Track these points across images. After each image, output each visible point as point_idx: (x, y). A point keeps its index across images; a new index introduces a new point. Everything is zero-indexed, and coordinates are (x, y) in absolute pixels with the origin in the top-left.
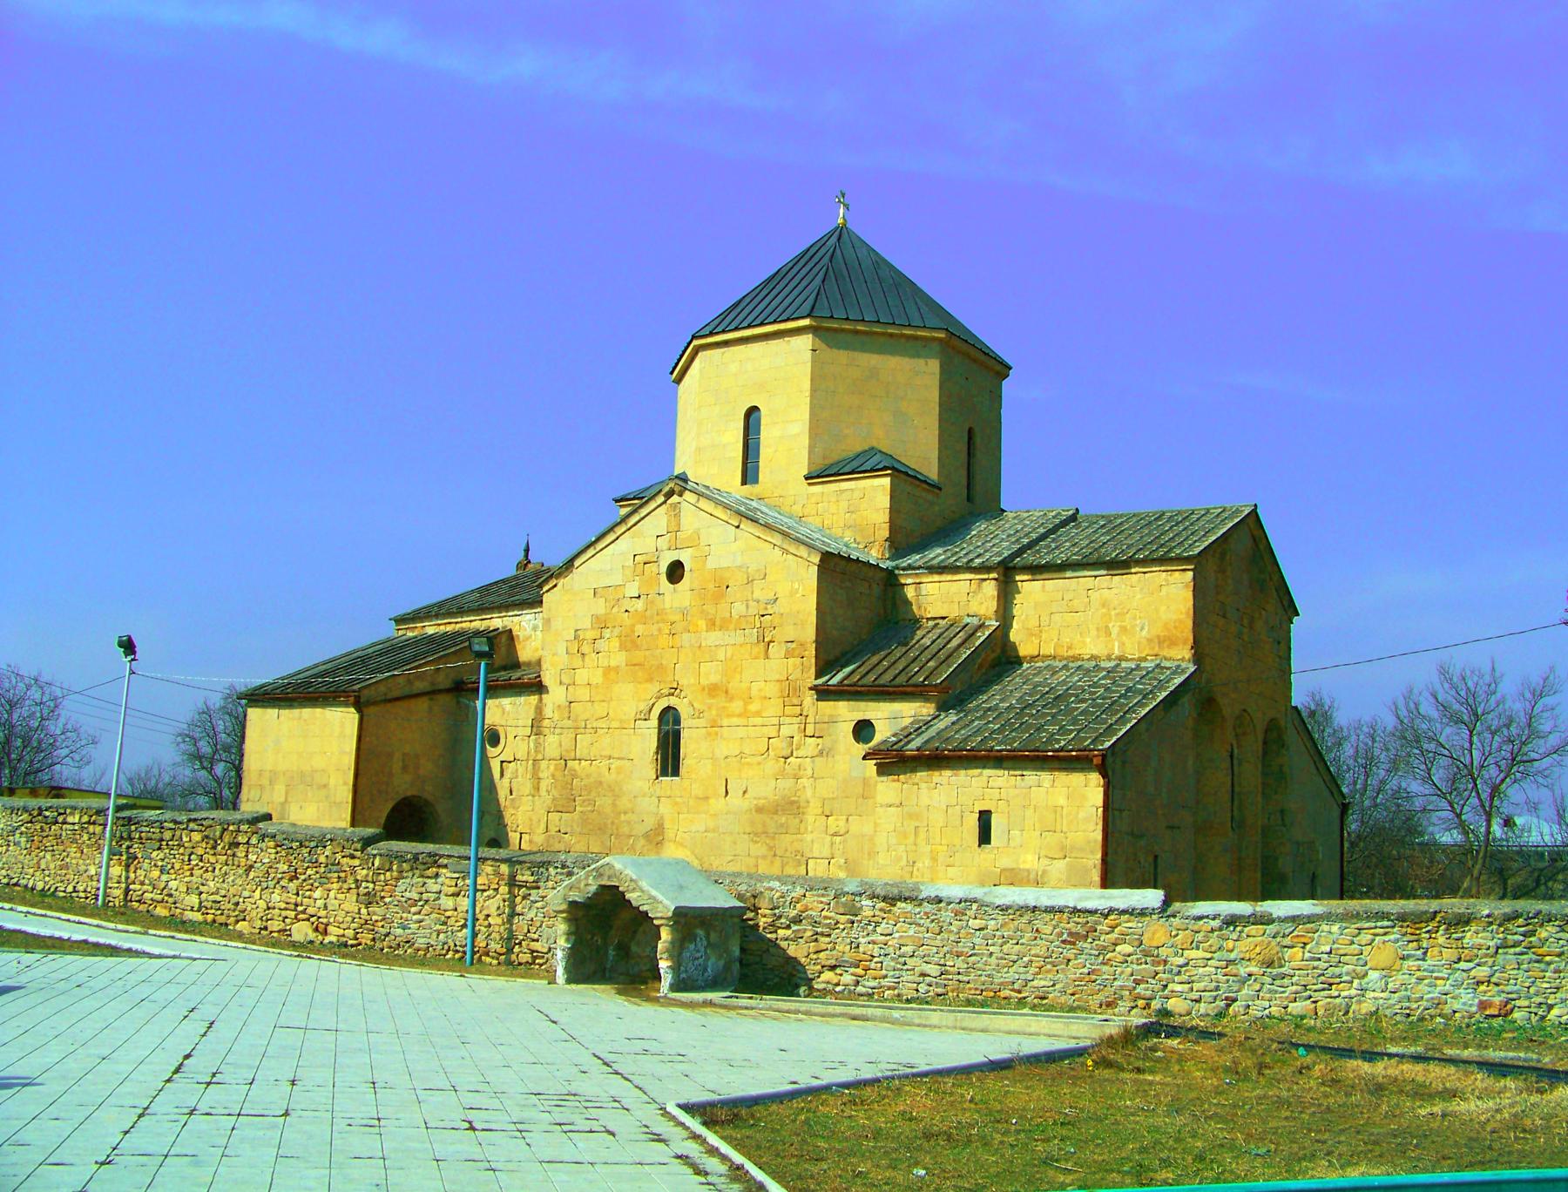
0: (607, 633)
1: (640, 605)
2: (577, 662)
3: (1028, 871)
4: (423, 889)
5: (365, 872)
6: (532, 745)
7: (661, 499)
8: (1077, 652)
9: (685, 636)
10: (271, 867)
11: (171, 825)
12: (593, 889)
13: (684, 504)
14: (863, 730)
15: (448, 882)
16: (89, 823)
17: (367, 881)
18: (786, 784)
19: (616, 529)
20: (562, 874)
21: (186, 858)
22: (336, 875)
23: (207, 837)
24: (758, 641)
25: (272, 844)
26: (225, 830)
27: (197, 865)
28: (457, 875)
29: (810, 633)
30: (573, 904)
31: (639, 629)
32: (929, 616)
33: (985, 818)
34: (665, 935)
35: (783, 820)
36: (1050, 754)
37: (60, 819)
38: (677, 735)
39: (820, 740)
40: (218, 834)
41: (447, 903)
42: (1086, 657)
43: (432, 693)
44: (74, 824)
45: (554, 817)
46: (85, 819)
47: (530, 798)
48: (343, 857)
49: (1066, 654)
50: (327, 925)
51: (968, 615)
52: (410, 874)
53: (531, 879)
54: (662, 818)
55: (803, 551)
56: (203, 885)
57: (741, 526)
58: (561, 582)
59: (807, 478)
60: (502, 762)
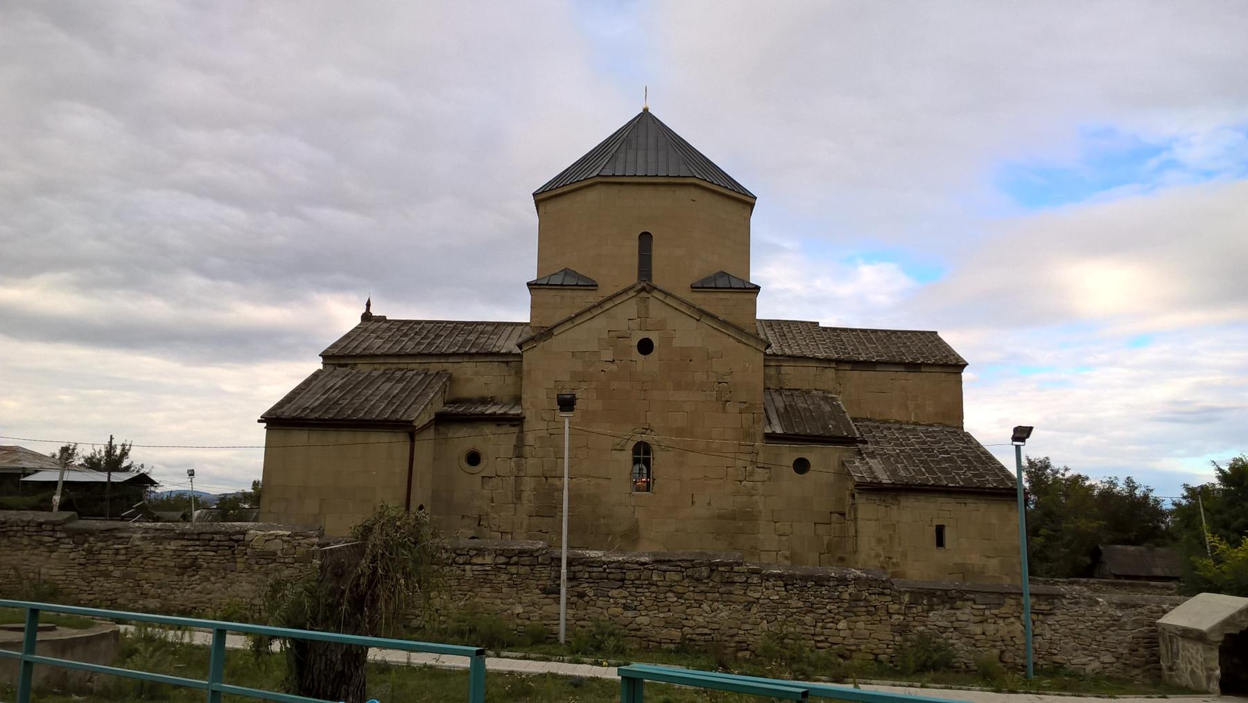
0: (584, 386)
1: (614, 367)
4: (954, 619)
5: (897, 606)
6: (513, 464)
7: (632, 294)
8: (886, 418)
10: (781, 603)
11: (636, 566)
13: (652, 299)
14: (801, 466)
15: (975, 612)
16: (507, 564)
17: (899, 614)
19: (592, 310)
20: (1071, 603)
21: (662, 596)
22: (865, 609)
23: (687, 577)
24: (717, 400)
25: (781, 583)
27: (677, 601)
28: (984, 607)
30: (1228, 636)
31: (615, 385)
32: (787, 388)
33: (940, 531)
35: (741, 524)
36: (987, 490)
37: (460, 560)
39: (768, 471)
40: (705, 574)
41: (978, 629)
42: (892, 421)
44: (483, 565)
45: (535, 520)
46: (502, 559)
47: (512, 505)
48: (870, 594)
49: (878, 419)
50: (851, 651)
51: (816, 390)
52: (941, 607)
53: (1048, 608)
54: (637, 521)
55: (752, 342)
56: (686, 619)
57: (702, 320)
59: (692, 287)
60: (483, 477)
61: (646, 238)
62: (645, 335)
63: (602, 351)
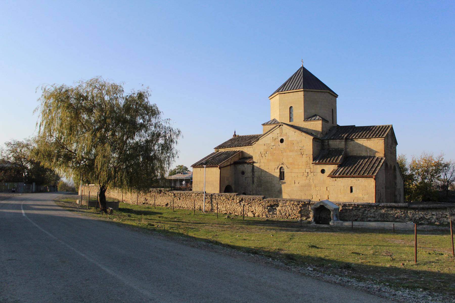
3: (360, 197)
9: (285, 153)
12: (319, 205)
14: (323, 171)
18: (307, 181)
26: (230, 197)
31: (275, 152)
33: (351, 188)
34: (332, 213)
37: (190, 195)
40: (229, 197)
43: (230, 165)
45: (257, 188)
58: (256, 142)
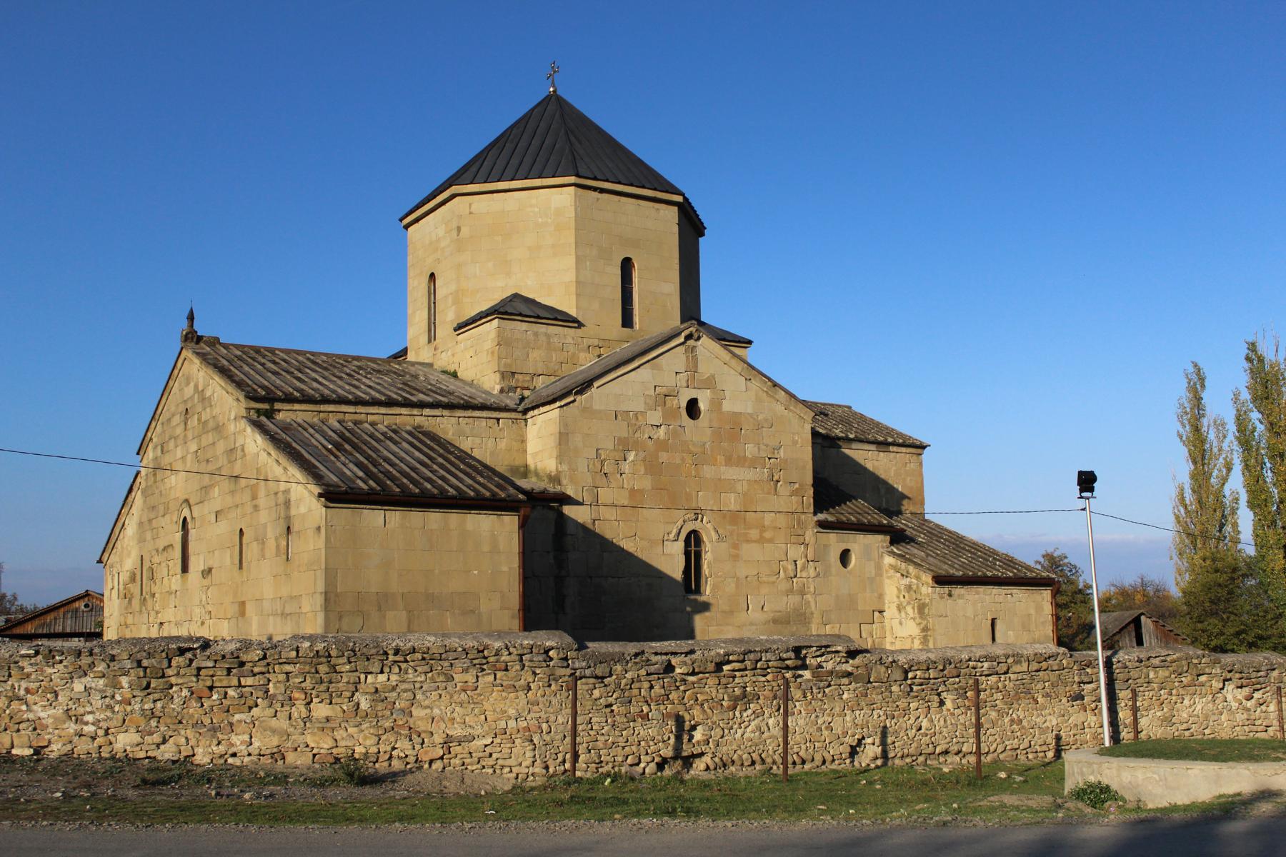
2: (601, 481)
18: (794, 600)
29: (809, 479)
31: (663, 457)
38: (698, 556)
46: (1035, 666)
58: (579, 398)
61: (627, 265)
62: (693, 394)
63: (649, 412)
